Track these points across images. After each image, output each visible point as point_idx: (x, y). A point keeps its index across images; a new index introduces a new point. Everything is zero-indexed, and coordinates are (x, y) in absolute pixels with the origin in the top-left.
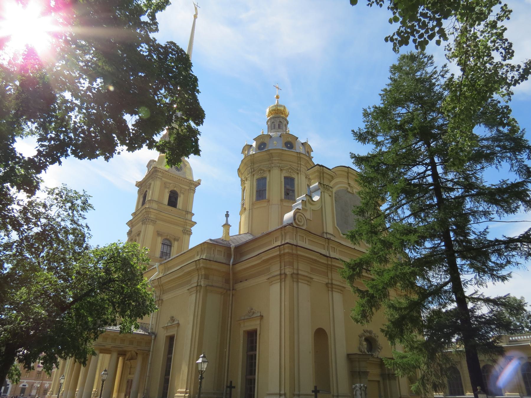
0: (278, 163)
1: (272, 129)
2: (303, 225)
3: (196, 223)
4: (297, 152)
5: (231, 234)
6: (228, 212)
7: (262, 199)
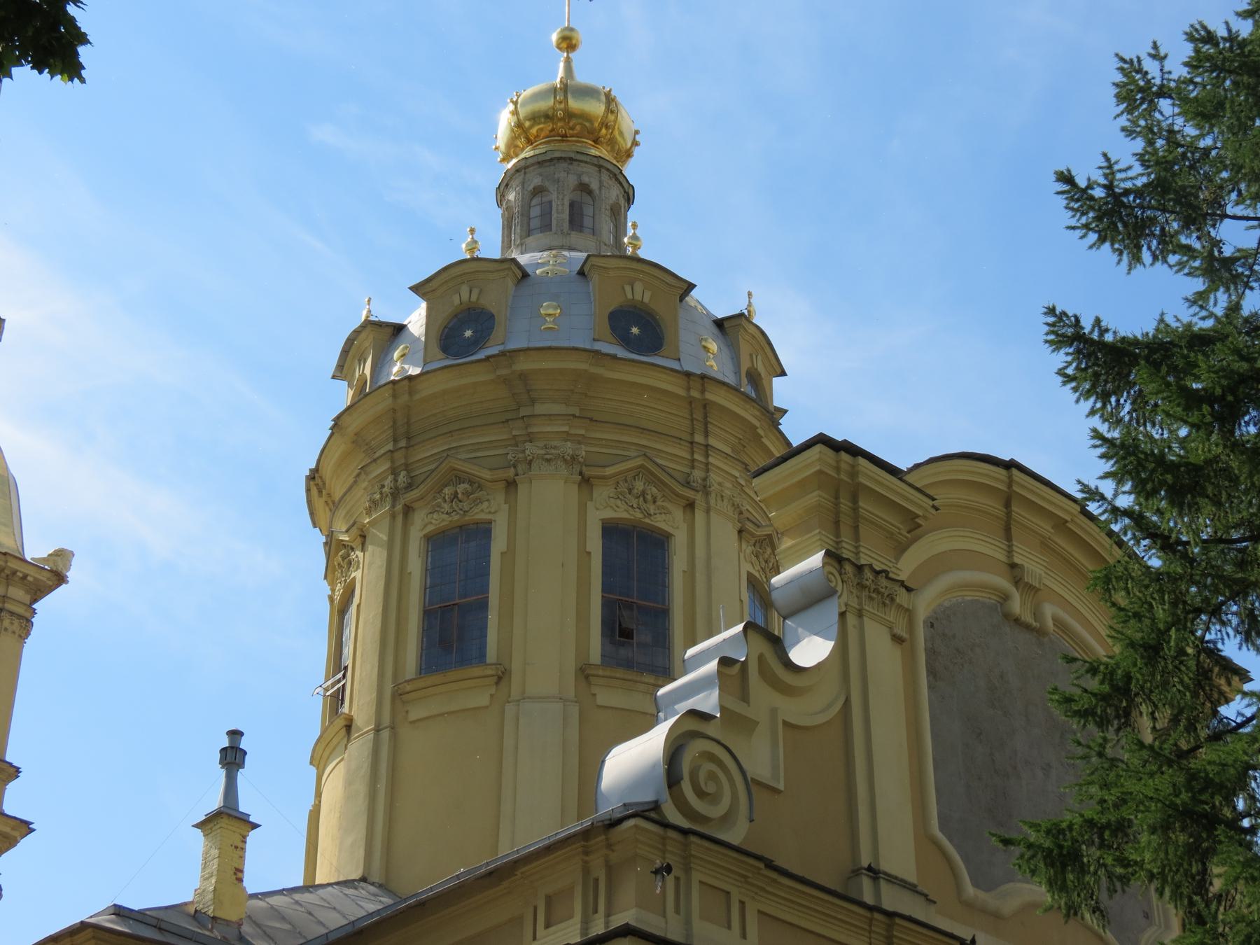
0: (567, 436)
1: (529, 233)
2: (727, 819)
3: (25, 827)
4: (688, 375)
5: (253, 884)
6: (235, 734)
7: (464, 662)
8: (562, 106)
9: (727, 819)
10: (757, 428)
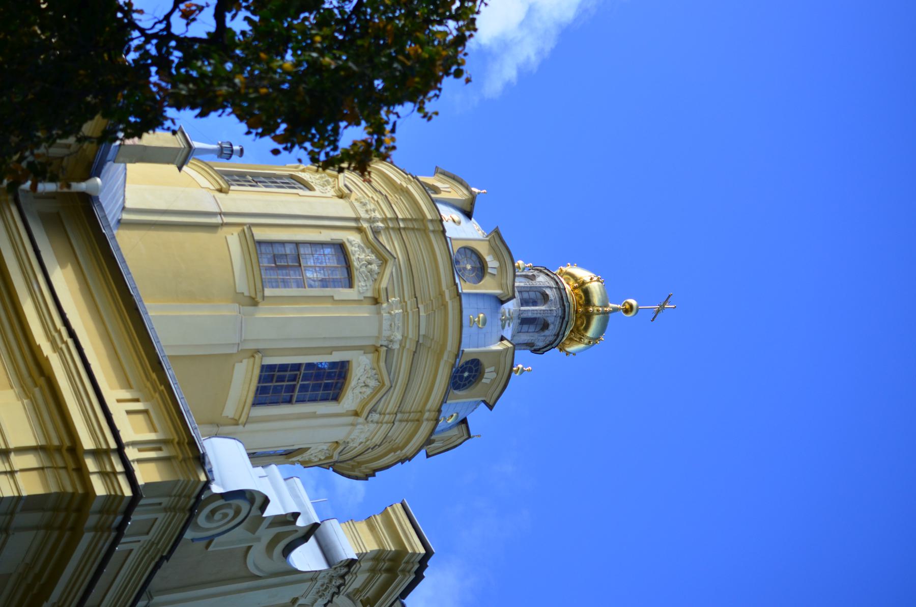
0: (405, 337)
8: (595, 311)
9: (198, 528)
10: (401, 451)
